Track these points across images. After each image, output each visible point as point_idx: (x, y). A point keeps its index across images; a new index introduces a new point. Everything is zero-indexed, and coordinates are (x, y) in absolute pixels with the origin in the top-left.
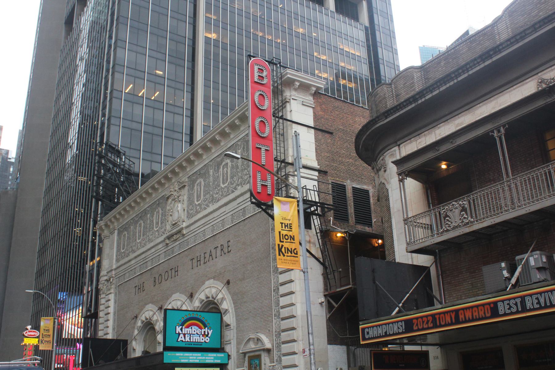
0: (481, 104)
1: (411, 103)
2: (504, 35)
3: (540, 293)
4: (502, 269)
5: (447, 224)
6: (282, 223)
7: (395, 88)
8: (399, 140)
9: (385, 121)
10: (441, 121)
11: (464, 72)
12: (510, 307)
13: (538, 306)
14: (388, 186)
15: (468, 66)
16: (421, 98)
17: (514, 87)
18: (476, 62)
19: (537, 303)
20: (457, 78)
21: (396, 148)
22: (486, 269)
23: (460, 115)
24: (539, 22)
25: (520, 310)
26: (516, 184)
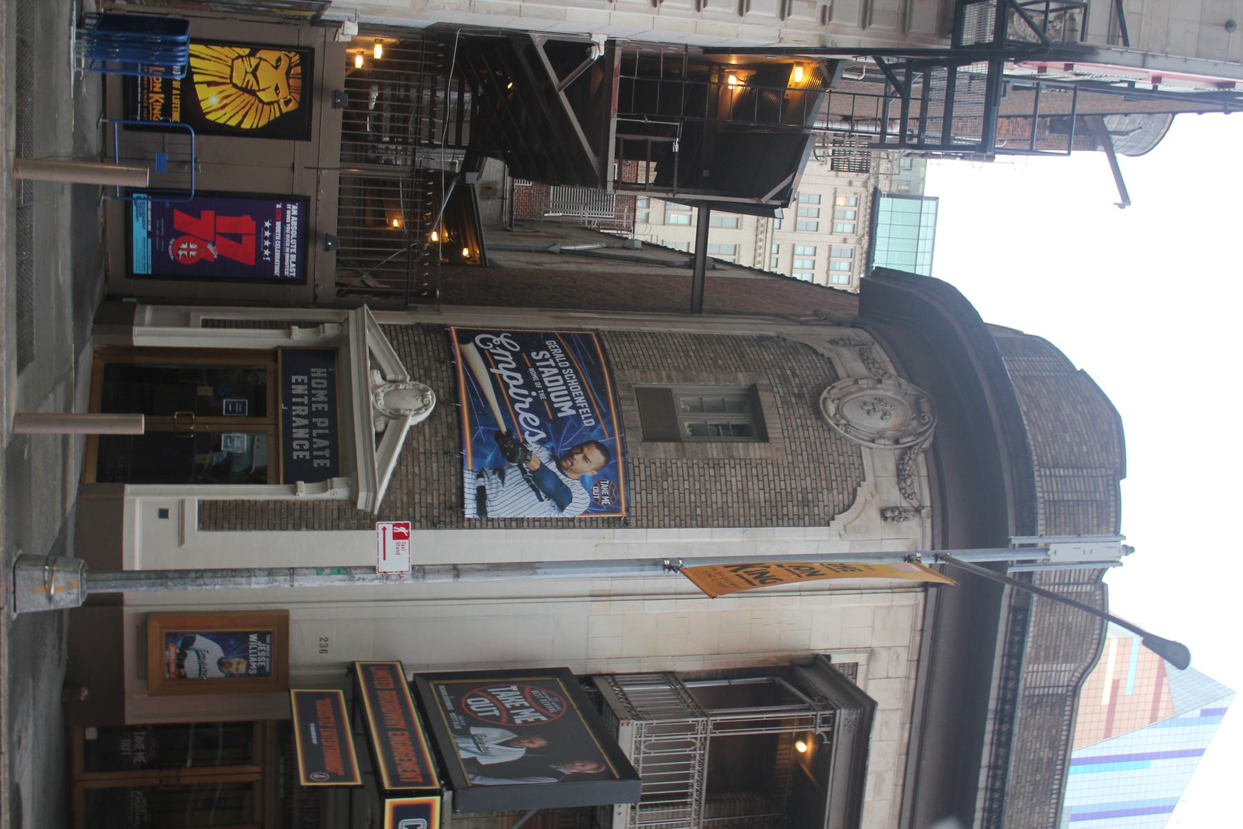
1: (1002, 700)
9: (1005, 602)
14: (841, 519)
23: (899, 789)
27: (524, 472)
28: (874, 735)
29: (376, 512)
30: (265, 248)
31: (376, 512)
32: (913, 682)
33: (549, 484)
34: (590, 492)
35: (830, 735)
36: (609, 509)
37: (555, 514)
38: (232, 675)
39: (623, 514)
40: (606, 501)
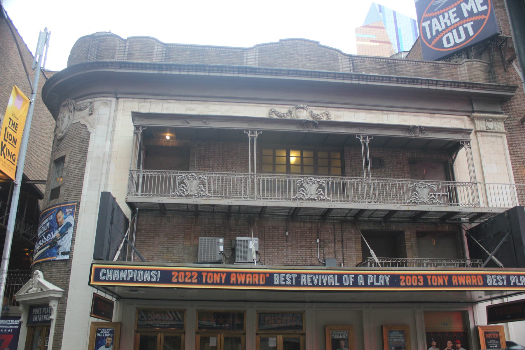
0: (216, 103)
1: (154, 69)
2: (251, 62)
3: (315, 274)
4: (219, 244)
5: (181, 190)
6: (11, 119)
7: (129, 46)
8: (120, 93)
9: (118, 71)
10: (173, 98)
11: (218, 71)
12: (285, 280)
13: (311, 284)
14: (89, 129)
15: (224, 69)
16: (167, 69)
17: (251, 104)
18: (232, 69)
19: (310, 282)
20: (209, 72)
21: (114, 100)
22: (202, 240)
24: (294, 71)
25: (294, 284)
26: (259, 180)
27: (60, 239)
28: (172, 112)
29: (63, 290)
30: (7, 331)
31: (63, 290)
32: (152, 100)
33: (64, 230)
34: (68, 215)
35: (143, 127)
36: (74, 209)
37: (72, 228)
38: (112, 343)
39: (76, 204)
40: (71, 210)
